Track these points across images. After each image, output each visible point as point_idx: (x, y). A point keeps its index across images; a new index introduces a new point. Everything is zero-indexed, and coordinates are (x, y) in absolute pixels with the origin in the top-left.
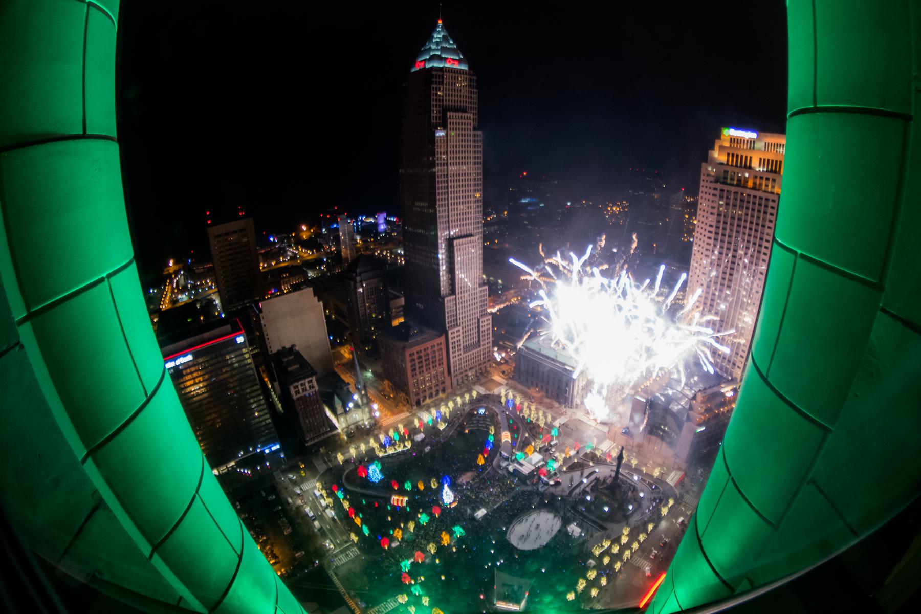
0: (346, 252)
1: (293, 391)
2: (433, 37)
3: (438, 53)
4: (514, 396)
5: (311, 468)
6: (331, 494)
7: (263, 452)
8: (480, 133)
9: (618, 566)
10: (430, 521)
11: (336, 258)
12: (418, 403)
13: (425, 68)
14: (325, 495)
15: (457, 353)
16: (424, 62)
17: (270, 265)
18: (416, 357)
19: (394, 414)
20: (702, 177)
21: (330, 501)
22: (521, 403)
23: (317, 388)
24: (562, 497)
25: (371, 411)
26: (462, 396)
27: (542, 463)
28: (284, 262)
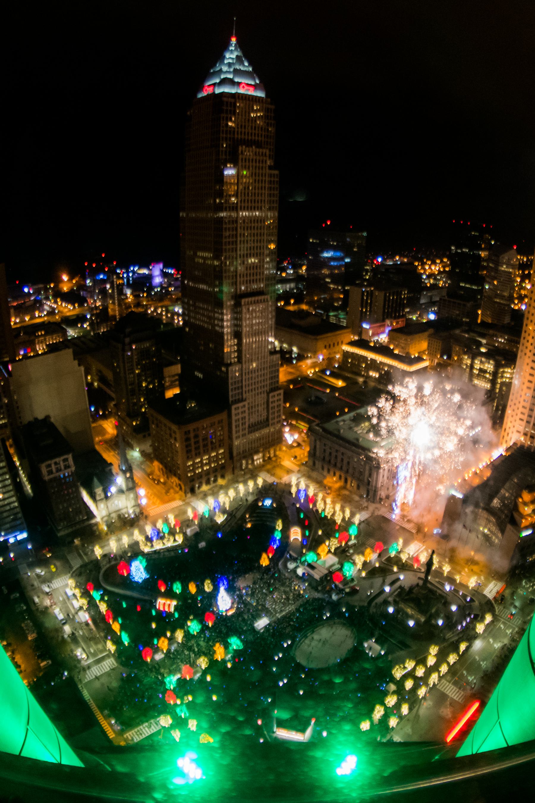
0: (114, 309)
1: (44, 470)
2: (224, 57)
3: (230, 76)
4: (307, 486)
6: (86, 594)
8: (276, 172)
9: (422, 692)
10: (202, 631)
11: (102, 315)
12: (192, 491)
13: (214, 93)
14: (78, 595)
15: (241, 433)
16: (213, 87)
18: (192, 435)
19: (164, 502)
21: (83, 602)
22: (315, 495)
23: (73, 469)
25: (137, 497)
26: (245, 483)
27: (337, 566)
28: (40, 317)
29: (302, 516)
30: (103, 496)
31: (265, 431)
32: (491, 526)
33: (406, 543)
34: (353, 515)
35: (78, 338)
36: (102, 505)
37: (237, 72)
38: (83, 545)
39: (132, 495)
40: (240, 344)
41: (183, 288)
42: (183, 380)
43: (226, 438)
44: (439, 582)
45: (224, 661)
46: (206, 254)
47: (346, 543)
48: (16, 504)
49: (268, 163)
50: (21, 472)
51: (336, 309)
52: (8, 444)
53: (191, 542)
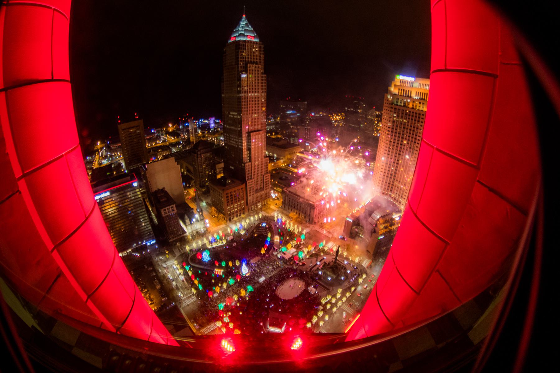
0: (193, 139)
1: (163, 212)
3: (243, 32)
4: (282, 217)
5: (172, 252)
6: (183, 267)
8: (265, 75)
9: (334, 310)
10: (235, 283)
11: (188, 142)
12: (230, 220)
14: (179, 268)
16: (236, 37)
17: (152, 145)
18: (229, 195)
19: (217, 225)
20: (385, 101)
21: (181, 271)
22: (285, 221)
23: (176, 211)
24: (306, 271)
25: (205, 223)
27: (296, 253)
30: (189, 223)
31: (262, 193)
33: (327, 243)
34: (303, 230)
35: (177, 152)
36: (189, 227)
37: (246, 30)
39: (202, 223)
41: (224, 129)
42: (225, 170)
45: (245, 297)
48: (150, 228)
51: (293, 137)
53: (230, 243)
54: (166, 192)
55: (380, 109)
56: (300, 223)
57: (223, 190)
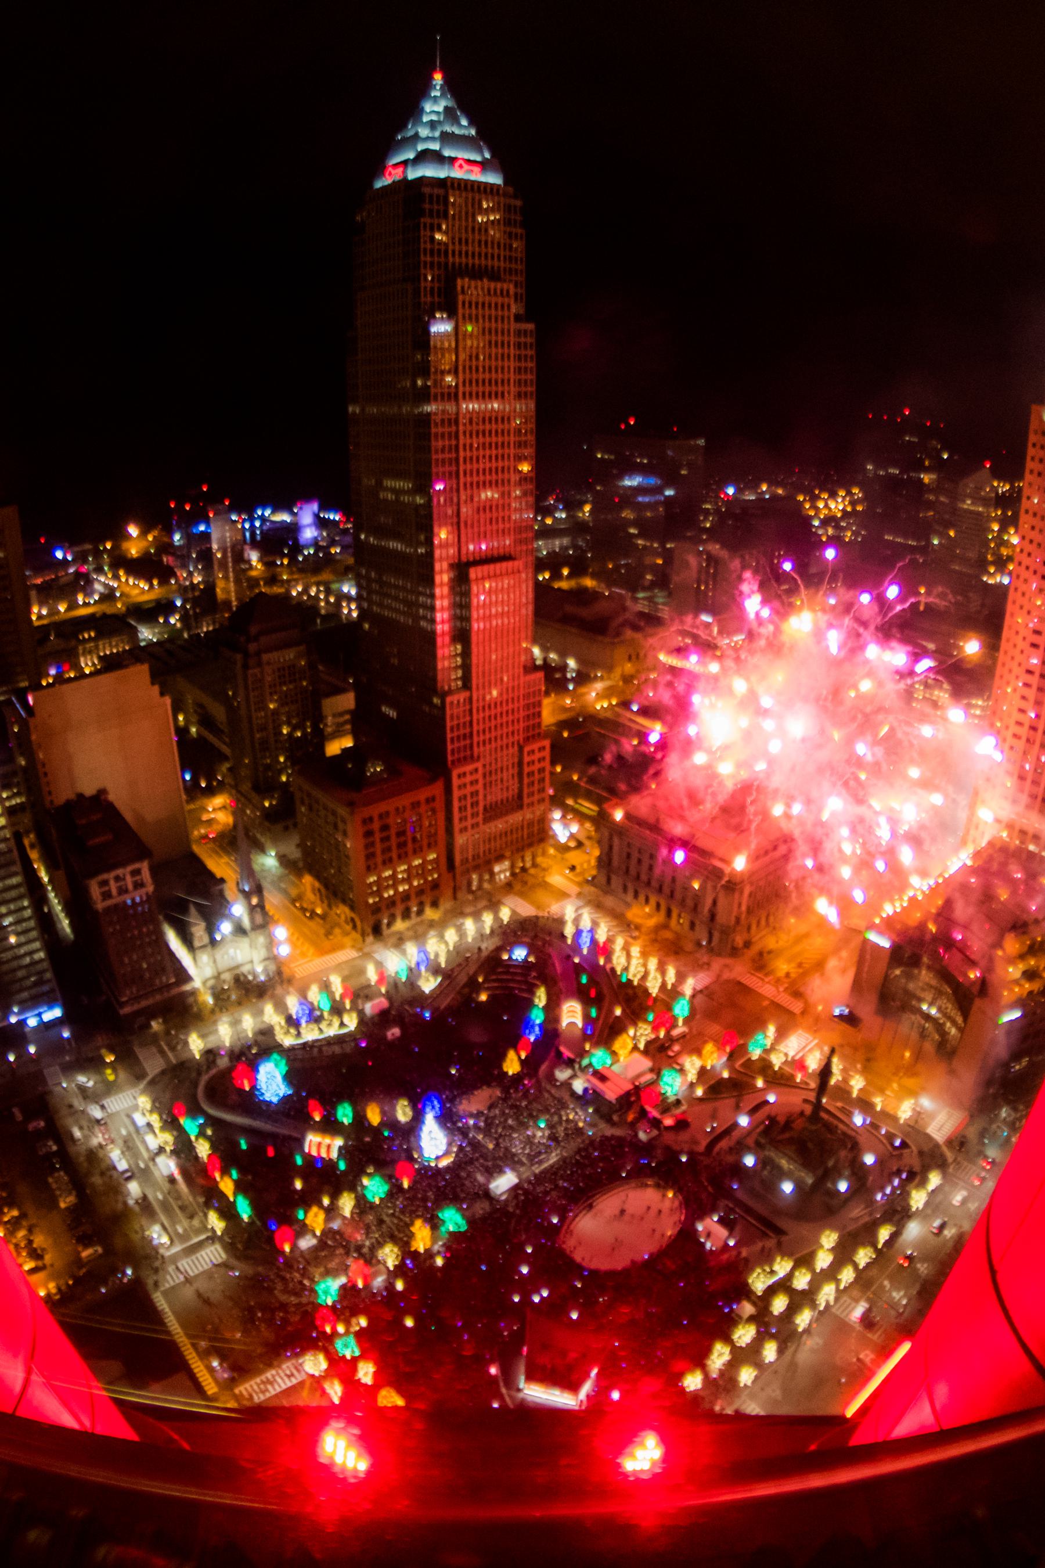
0: (226, 589)
1: (95, 891)
2: (422, 111)
3: (435, 146)
4: (595, 924)
5: (127, 1058)
6: (171, 1123)
7: (22, 1023)
8: (530, 326)
9: (803, 1319)
10: (391, 1195)
11: (204, 600)
12: (377, 931)
14: (157, 1124)
15: (470, 822)
16: (402, 167)
17: (53, 612)
18: (376, 826)
19: (322, 952)
21: (167, 1138)
22: (610, 940)
23: (150, 888)
24: (691, 1154)
25: (271, 943)
26: (477, 916)
27: (649, 1077)
28: (86, 605)
29: (584, 980)
30: (206, 940)
31: (516, 818)
32: (943, 1002)
33: (781, 1034)
34: (681, 977)
35: (158, 643)
36: (204, 958)
37: (447, 138)
38: (167, 1033)
39: (261, 940)
40: (466, 654)
41: (358, 549)
42: (361, 721)
43: (442, 832)
44: (842, 1110)
45: (430, 1254)
46: (399, 484)
47: (668, 1032)
48: (42, 955)
49: (513, 310)
50: (52, 895)
52: (26, 842)
53: (373, 1027)
54: (111, 806)
55: (1011, 467)
56: (669, 947)
57: (351, 805)
